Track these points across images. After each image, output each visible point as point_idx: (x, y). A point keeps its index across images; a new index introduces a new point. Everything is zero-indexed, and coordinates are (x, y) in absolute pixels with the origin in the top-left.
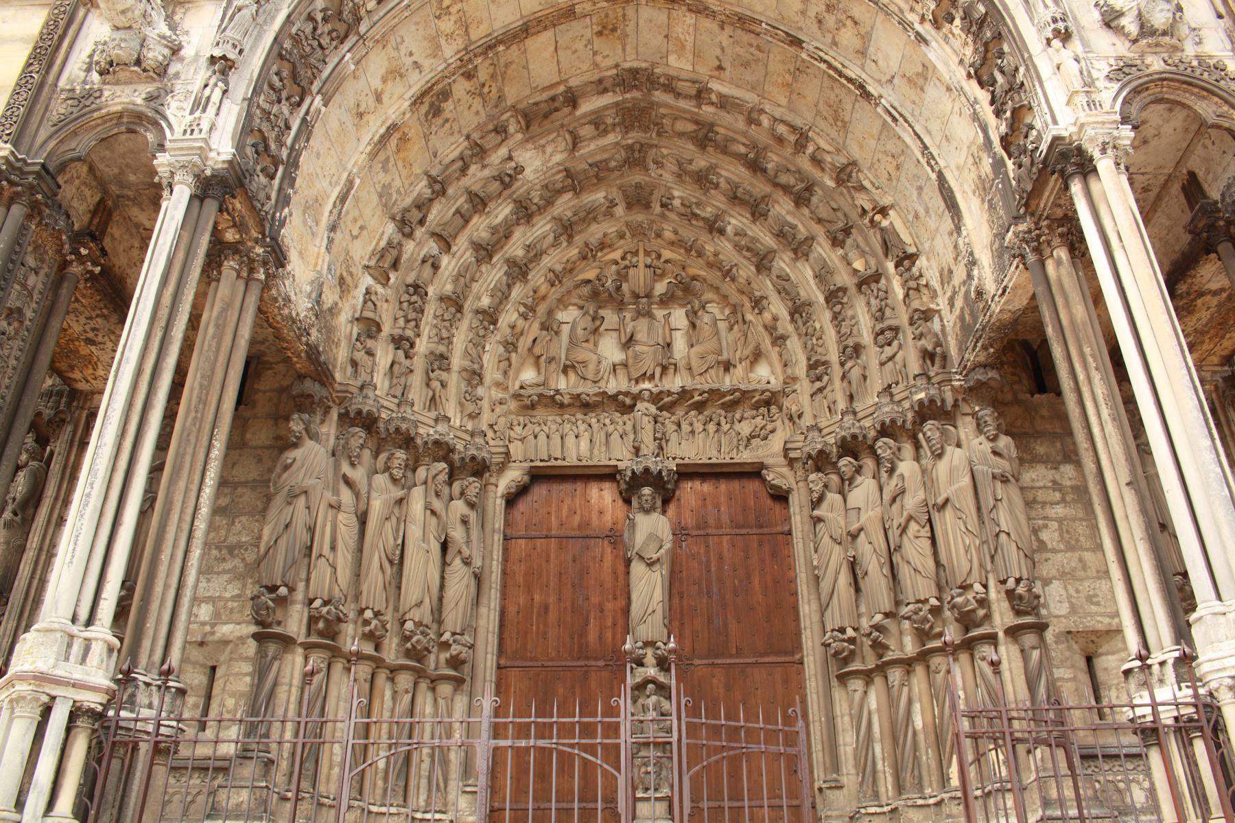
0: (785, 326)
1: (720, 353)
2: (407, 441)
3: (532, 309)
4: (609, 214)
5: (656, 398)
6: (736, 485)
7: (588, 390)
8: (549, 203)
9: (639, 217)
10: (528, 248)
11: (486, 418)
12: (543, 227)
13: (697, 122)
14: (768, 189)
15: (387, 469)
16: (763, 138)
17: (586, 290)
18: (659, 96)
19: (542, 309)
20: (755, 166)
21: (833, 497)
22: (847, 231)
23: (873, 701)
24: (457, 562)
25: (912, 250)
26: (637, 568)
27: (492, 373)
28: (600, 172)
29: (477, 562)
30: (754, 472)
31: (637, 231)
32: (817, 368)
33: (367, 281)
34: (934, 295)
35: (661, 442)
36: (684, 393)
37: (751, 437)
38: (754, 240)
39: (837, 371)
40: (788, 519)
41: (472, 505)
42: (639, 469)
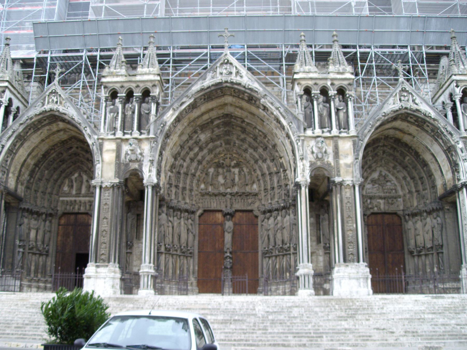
0: (260, 177)
1: (245, 182)
2: (179, 210)
3: (203, 171)
4: (221, 146)
5: (231, 194)
6: (247, 213)
7: (216, 192)
8: (207, 146)
9: (228, 146)
10: (202, 157)
11: (194, 199)
12: (205, 151)
15: (176, 216)
16: (257, 134)
17: (215, 165)
19: (205, 170)
20: (255, 139)
21: (266, 220)
22: (273, 160)
23: (270, 262)
24: (190, 233)
26: (226, 234)
27: (195, 188)
28: (219, 137)
29: (194, 233)
30: (251, 211)
31: (228, 150)
33: (169, 173)
34: (289, 180)
35: (232, 205)
38: (254, 156)
39: (269, 192)
40: (257, 222)
41: (192, 221)
42: (227, 212)
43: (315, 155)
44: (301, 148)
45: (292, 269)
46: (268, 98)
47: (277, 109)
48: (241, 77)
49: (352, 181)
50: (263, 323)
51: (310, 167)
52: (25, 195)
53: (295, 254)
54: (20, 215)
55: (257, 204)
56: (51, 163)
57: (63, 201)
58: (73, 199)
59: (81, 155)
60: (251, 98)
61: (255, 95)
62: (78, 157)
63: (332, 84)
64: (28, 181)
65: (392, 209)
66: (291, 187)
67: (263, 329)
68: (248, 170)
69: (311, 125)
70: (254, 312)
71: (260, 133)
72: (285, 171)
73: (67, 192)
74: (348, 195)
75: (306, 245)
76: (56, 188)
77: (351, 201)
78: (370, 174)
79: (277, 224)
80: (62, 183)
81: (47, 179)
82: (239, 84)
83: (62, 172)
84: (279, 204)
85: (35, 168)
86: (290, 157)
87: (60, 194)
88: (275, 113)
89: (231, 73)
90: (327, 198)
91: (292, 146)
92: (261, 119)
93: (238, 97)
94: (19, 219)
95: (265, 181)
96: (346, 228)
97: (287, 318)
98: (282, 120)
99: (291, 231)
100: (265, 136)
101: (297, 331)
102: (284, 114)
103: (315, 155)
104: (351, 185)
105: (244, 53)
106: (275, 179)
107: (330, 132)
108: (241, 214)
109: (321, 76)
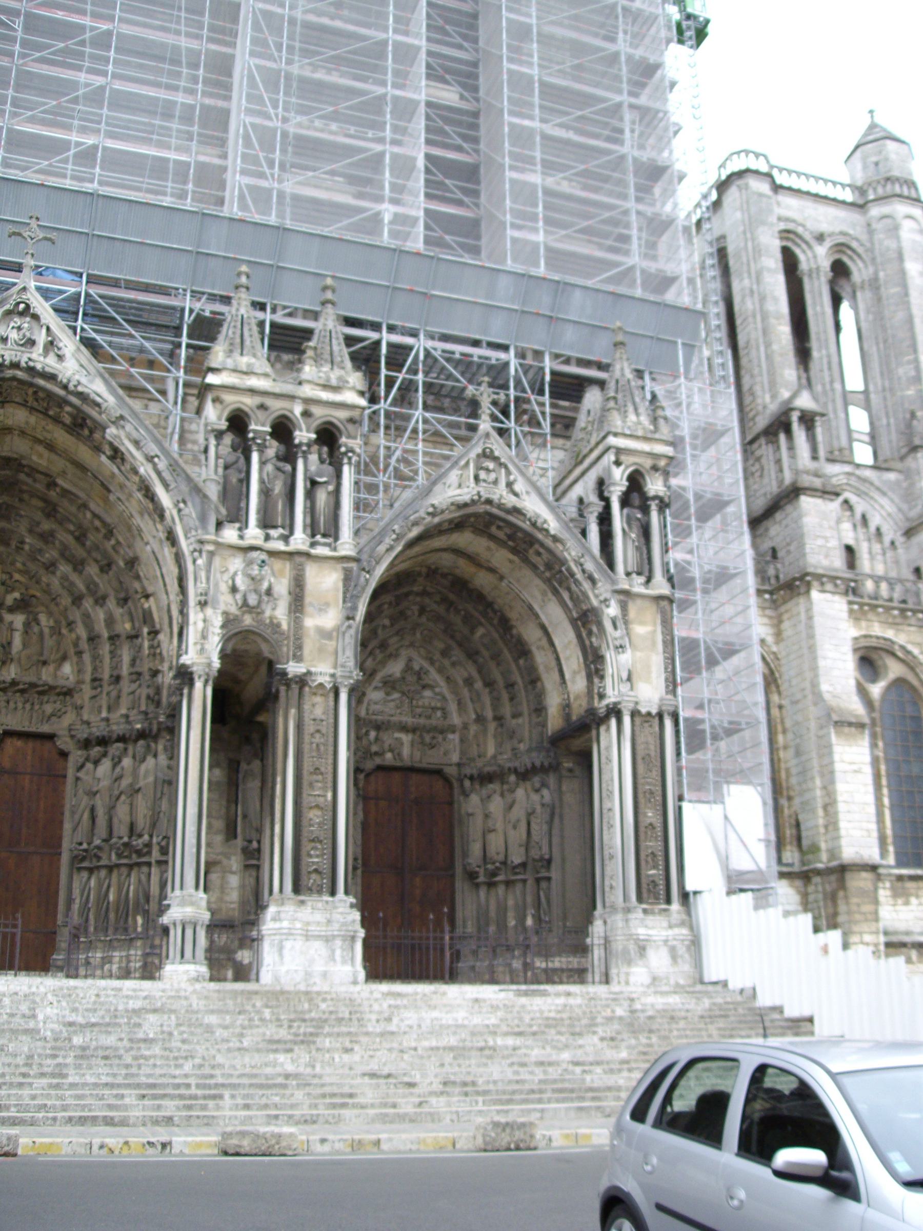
0: (84, 645)
1: (41, 654)
6: (38, 743)
13: (45, 501)
14: (85, 555)
18: (22, 476)
20: (81, 538)
21: (89, 766)
22: (125, 600)
23: (93, 883)
25: (158, 626)
30: (51, 737)
32: (96, 681)
34: (162, 660)
36: (14, 683)
37: (53, 715)
38: (72, 584)
39: (106, 688)
40: (65, 768)
43: (239, 596)
44: (203, 574)
45: (153, 906)
46: (128, 427)
47: (150, 459)
48: (60, 358)
49: (333, 676)
50: (55, 1056)
51: (223, 627)
53: (162, 863)
55: (69, 718)
60: (82, 421)
61: (93, 413)
63: (306, 414)
65: (432, 759)
66: (167, 678)
67: (53, 1075)
68: (52, 623)
69: (237, 516)
70: (32, 1025)
71: (97, 523)
72: (154, 633)
74: (319, 712)
75: (194, 841)
77: (324, 731)
78: (383, 663)
79: (119, 778)
82: (52, 377)
84: (128, 722)
86: (172, 597)
88: (142, 470)
89: (32, 343)
90: (261, 718)
91: (180, 567)
92: (103, 484)
93: (45, 414)
95: (96, 658)
96: (306, 800)
97: (125, 1042)
98: (159, 490)
99: (157, 800)
100: (110, 534)
101: (151, 1081)
102: (167, 475)
103: (239, 596)
104: (329, 686)
105: (79, 294)
106: (126, 656)
107: (286, 539)
108: (19, 743)
109: (278, 388)
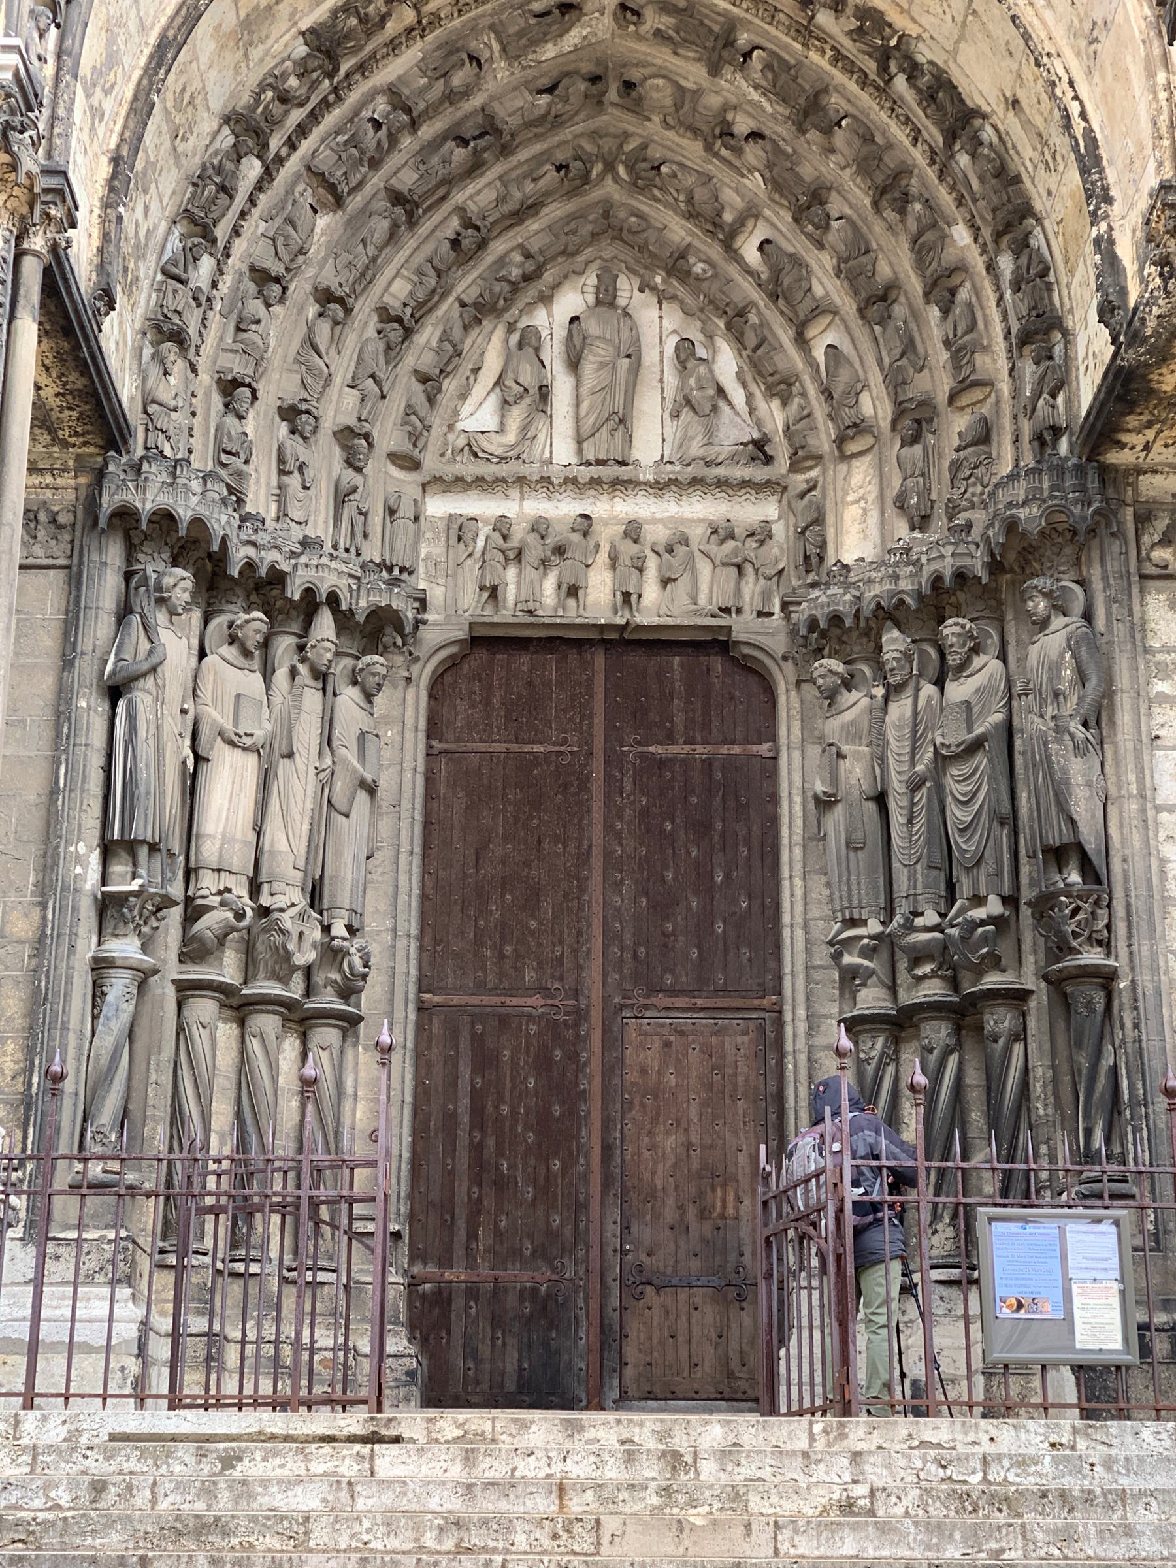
52: (148, 400)
54: (107, 588)
56: (370, 138)
57: (460, 530)
58: (563, 509)
59: (659, 93)
62: (614, 118)
64: (173, 275)
73: (495, 445)
76: (404, 390)
80: (451, 355)
81: (326, 297)
83: (467, 245)
85: (237, 154)
87: (431, 463)
94: (99, 627)
